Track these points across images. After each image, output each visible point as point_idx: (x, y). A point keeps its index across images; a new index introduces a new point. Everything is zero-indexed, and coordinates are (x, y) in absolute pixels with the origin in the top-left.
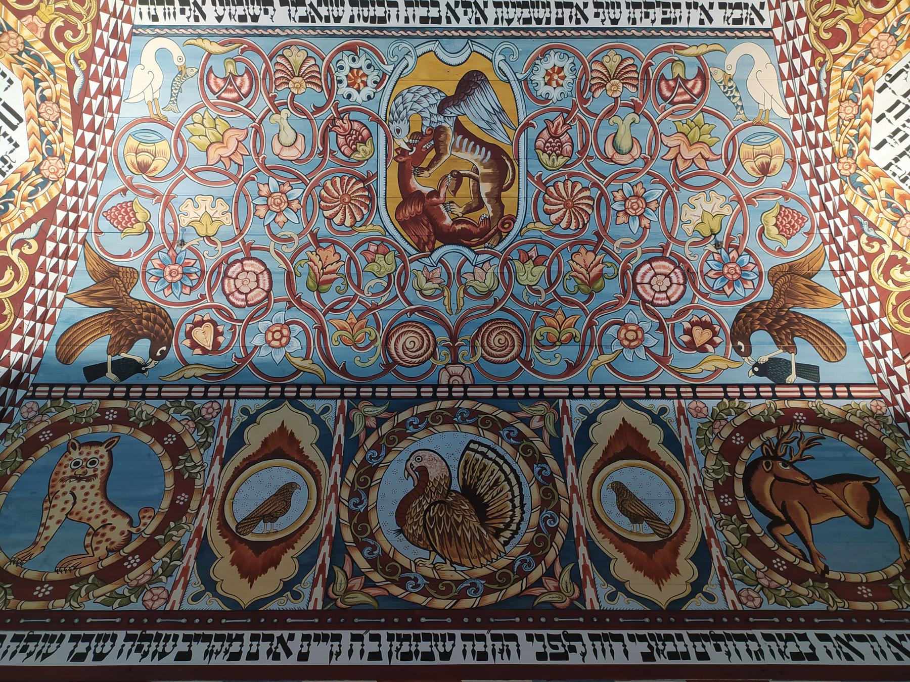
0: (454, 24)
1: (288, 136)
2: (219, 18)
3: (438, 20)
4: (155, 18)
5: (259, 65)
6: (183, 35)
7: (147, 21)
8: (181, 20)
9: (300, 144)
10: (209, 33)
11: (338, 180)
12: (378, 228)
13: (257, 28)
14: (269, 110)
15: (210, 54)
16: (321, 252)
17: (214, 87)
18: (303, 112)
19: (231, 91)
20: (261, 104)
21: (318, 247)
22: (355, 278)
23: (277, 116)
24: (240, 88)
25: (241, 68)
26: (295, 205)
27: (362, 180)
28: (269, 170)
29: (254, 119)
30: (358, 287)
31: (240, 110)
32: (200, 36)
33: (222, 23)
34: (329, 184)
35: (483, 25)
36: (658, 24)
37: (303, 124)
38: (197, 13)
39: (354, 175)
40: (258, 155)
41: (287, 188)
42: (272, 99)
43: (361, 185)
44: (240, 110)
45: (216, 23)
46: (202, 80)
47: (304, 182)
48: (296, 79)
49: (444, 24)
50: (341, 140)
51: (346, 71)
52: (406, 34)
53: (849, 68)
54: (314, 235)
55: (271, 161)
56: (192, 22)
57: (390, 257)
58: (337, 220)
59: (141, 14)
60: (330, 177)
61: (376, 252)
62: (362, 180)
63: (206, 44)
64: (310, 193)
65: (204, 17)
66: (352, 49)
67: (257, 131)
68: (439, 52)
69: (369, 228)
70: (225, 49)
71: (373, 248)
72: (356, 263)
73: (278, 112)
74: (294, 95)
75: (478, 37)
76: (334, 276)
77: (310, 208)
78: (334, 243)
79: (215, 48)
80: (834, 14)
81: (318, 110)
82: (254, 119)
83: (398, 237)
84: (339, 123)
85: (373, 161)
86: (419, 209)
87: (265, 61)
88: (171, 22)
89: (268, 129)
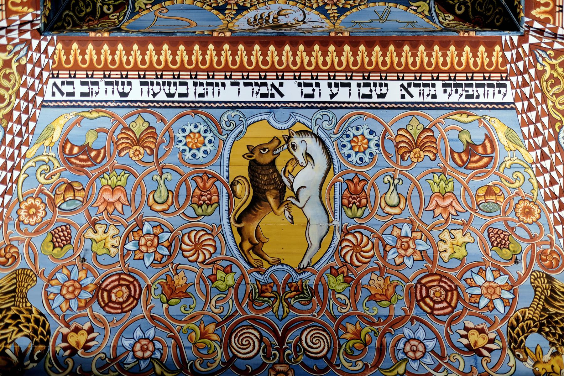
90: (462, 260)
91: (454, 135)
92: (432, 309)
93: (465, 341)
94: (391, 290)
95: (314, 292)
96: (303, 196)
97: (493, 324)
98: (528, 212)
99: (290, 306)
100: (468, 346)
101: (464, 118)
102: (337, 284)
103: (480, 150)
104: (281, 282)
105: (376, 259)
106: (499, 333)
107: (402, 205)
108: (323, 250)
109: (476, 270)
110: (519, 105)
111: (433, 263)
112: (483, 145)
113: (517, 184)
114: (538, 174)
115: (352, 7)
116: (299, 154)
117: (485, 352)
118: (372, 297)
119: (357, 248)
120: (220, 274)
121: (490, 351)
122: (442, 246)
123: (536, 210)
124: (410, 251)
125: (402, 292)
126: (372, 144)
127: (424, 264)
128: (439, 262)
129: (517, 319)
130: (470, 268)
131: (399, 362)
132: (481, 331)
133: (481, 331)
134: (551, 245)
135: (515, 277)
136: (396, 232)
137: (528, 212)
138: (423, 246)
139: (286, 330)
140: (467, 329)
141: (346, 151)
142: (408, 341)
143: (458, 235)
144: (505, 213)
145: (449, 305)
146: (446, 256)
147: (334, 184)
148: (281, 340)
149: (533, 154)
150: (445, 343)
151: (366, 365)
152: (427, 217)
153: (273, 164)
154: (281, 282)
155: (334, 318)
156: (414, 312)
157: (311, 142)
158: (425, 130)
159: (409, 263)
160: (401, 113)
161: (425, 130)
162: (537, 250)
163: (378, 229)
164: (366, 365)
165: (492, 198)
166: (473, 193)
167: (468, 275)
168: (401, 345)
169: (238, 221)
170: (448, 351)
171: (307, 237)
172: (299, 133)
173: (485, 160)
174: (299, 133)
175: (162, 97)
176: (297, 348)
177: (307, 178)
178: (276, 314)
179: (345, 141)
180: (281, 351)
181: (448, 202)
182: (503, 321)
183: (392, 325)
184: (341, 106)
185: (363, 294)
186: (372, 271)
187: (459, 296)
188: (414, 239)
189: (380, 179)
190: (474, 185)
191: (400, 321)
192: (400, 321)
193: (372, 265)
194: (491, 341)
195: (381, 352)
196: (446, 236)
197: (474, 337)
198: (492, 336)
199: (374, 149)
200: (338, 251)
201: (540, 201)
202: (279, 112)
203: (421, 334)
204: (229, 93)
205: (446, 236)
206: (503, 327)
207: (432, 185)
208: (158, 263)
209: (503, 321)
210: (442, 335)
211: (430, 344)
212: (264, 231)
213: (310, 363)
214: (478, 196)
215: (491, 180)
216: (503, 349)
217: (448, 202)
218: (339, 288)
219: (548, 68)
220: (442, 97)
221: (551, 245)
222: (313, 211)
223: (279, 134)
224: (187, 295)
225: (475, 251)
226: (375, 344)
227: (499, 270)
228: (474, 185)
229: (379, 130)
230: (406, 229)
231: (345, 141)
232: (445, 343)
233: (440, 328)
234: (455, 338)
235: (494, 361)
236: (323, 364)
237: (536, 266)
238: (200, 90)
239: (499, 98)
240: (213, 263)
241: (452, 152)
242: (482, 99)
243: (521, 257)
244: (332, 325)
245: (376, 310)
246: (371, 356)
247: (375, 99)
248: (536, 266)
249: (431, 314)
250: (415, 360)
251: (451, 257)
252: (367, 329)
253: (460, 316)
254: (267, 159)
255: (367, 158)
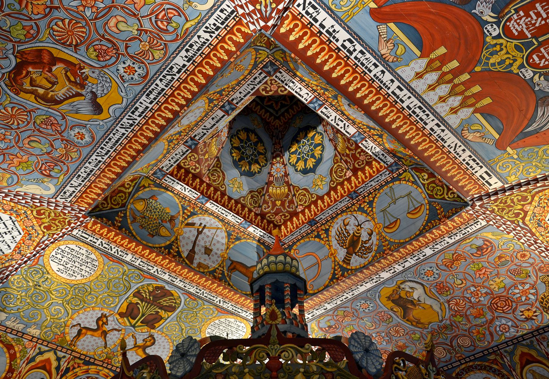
0: (127, 117)
1: (122, 26)
2: (199, 37)
3: (133, 113)
4: (222, 11)
5: (168, 37)
6: (205, 16)
7: (224, 6)
8: (212, 21)
9: (114, 29)
10: (196, 28)
11: (84, 35)
12: (44, 39)
13: (183, 48)
14: (142, 27)
15: (187, 21)
16: (43, 7)
17: (171, 11)
18: (130, 40)
19: (163, 17)
20: (147, 25)
21: (47, 7)
22: (16, 16)
23: (136, 28)
24: (162, 22)
25: (171, 29)
26: (81, 8)
27: (77, 45)
28: (110, 8)
29: (142, 17)
30: (9, 15)
31: (151, 14)
32: (199, 23)
33: (196, 36)
34: (83, 30)
35: (119, 125)
36: (79, 173)
37: (123, 36)
38: (209, 30)
39: (82, 43)
40: (122, 8)
41: (94, 10)
42: (146, 32)
43: (74, 43)
44: (151, 14)
45: (198, 34)
46: (179, 8)
47: (92, 20)
48: (148, 47)
49: (130, 114)
50: (104, 48)
51: (136, 69)
52: (136, 99)
53: (25, 212)
54: (57, 8)
55: (114, 12)
56: (207, 25)
57: (22, 37)
58: (60, 23)
59: (229, 6)
60: (88, 32)
61: (28, 32)
62: (77, 45)
63: (193, 23)
64: (84, 19)
65: (205, 32)
66: (145, 77)
67: (135, 15)
68: (120, 106)
69: (47, 36)
70: (184, 29)
71: (32, 32)
72: (26, 20)
73: (137, 30)
74: (141, 42)
75: (116, 121)
76: (23, 6)
77: (75, 14)
78: (46, 16)
79: (188, 25)
80: (49, 216)
81: (127, 47)
82: (142, 17)
83: (33, 45)
84: (114, 51)
85: (84, 54)
86: (45, 61)
87: (166, 41)
88: (214, 16)
89: (132, 20)
90: (505, 287)
91: (469, 248)
92: (503, 310)
93: (524, 317)
94: (481, 312)
95: (452, 325)
96: (422, 299)
97: (532, 305)
98: (524, 256)
99: (446, 334)
100: (526, 318)
101: (468, 241)
102: (458, 319)
103: (485, 246)
104: (437, 328)
105: (468, 304)
106: (536, 307)
107: (464, 282)
108: (444, 311)
109: (513, 288)
110: (491, 223)
111: (492, 294)
112: (485, 244)
113: (511, 248)
114: (519, 239)
115: (374, 198)
116: (407, 289)
117: (534, 318)
118: (475, 317)
119: (457, 304)
120: (413, 336)
121: (536, 316)
122: (492, 287)
123: (527, 253)
124: (480, 295)
125: (486, 310)
126: (434, 271)
127: (489, 296)
128: (494, 293)
129: (542, 298)
130: (510, 288)
131: (500, 336)
132: (528, 310)
133: (528, 310)
134: (543, 262)
135: (533, 283)
136: (469, 292)
137: (524, 256)
138: (484, 291)
139: (451, 342)
140: (522, 312)
141: (426, 278)
142: (500, 326)
143: (497, 279)
144: (513, 262)
145: (509, 306)
146: (496, 289)
147: (430, 290)
148: (452, 346)
149: (512, 234)
150: (516, 321)
151: (488, 342)
152: (479, 281)
153: (400, 297)
154: (437, 328)
155: (466, 330)
156: (496, 315)
157: (409, 284)
158: (453, 255)
159: (482, 299)
160: (438, 255)
161: (453, 255)
162: (537, 268)
163: (460, 295)
164: (488, 342)
165: (503, 259)
166: (493, 262)
167: (510, 291)
168: (498, 329)
169: (404, 318)
170: (518, 323)
171: (435, 311)
172: (401, 284)
173: (490, 248)
174: (401, 284)
175: (339, 303)
176: (459, 346)
177: (418, 294)
178: (443, 339)
179: (422, 276)
180: (455, 350)
181: (484, 271)
182: (536, 302)
183: (490, 323)
184: (410, 268)
185: (471, 318)
186: (469, 308)
187: (511, 301)
188: (478, 290)
189: (448, 279)
190: (490, 259)
191: (492, 321)
192: (492, 321)
193: (467, 307)
194: (535, 312)
195: (491, 334)
196: (492, 283)
197: (527, 314)
198: (534, 310)
199: (437, 272)
200: (450, 309)
201: (527, 249)
202: (387, 283)
203: (504, 321)
204: (362, 289)
205: (492, 283)
206: (538, 304)
207: (472, 269)
208: (388, 342)
209: (536, 302)
210: (513, 318)
211: (510, 324)
212: (416, 316)
213: (467, 349)
214: (496, 262)
215: (498, 254)
216: (542, 313)
217: (484, 271)
218: (460, 320)
219: (494, 207)
220: (451, 241)
221: (543, 262)
222: (429, 302)
223: (394, 288)
224: (407, 347)
225: (508, 281)
226: (487, 333)
227: (524, 283)
228: (490, 259)
229: (434, 265)
230: (472, 289)
231: (422, 276)
232: (516, 321)
233: (511, 316)
234: (518, 317)
235: (540, 319)
236: (472, 348)
237: (540, 274)
238: (351, 294)
239: (479, 226)
240: (407, 334)
241: (472, 254)
242: (471, 231)
243: (531, 274)
244: (467, 333)
245: (479, 321)
246: (489, 338)
247: (422, 258)
248: (540, 274)
249: (504, 312)
250: (506, 332)
251: (499, 288)
252: (481, 329)
253: (516, 308)
254: (397, 297)
255: (436, 276)
